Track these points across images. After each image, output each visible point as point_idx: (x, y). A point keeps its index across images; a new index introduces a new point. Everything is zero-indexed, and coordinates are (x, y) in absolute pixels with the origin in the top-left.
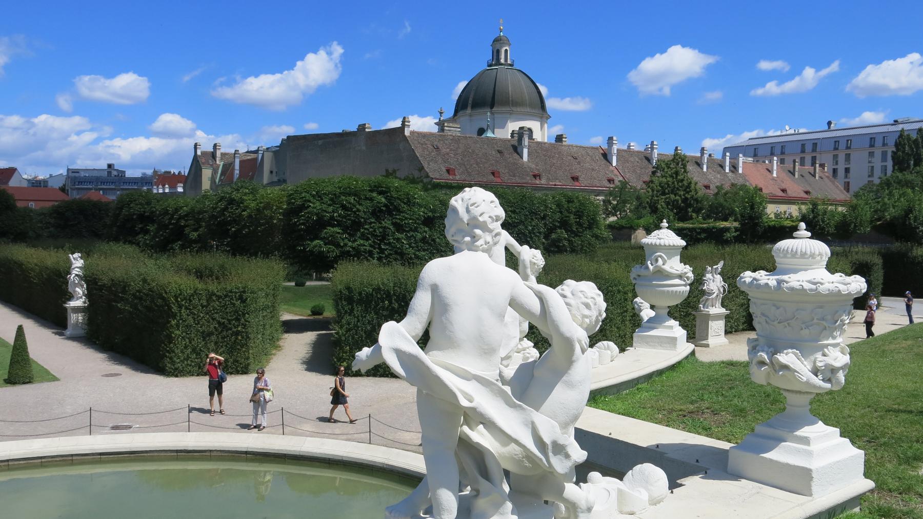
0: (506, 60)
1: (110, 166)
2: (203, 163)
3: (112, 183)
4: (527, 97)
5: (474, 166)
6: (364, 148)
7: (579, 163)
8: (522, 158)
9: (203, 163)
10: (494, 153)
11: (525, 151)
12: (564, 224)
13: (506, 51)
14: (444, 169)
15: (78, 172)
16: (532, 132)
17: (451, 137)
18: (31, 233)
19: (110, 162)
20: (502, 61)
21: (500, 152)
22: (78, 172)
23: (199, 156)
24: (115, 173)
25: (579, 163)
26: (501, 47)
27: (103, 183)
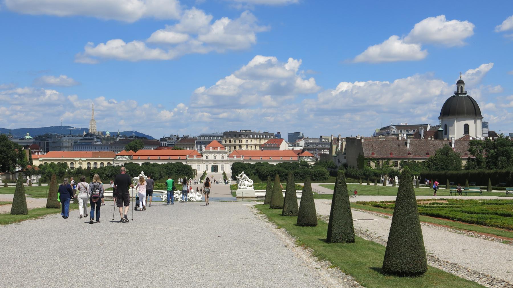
0: (462, 91)
1: (321, 137)
2: (333, 143)
3: (321, 145)
4: (466, 110)
5: (384, 151)
6: (356, 144)
7: (435, 148)
8: (407, 147)
9: (333, 143)
10: (396, 146)
11: (408, 145)
12: (315, 176)
13: (462, 87)
14: (371, 153)
15: (308, 140)
16: (468, 126)
17: (380, 141)
18: (250, 174)
19: (321, 135)
20: (459, 92)
21: (399, 145)
22: (308, 140)
23: (332, 140)
24: (323, 140)
25: (435, 148)
26: (459, 86)
27: (317, 145)
